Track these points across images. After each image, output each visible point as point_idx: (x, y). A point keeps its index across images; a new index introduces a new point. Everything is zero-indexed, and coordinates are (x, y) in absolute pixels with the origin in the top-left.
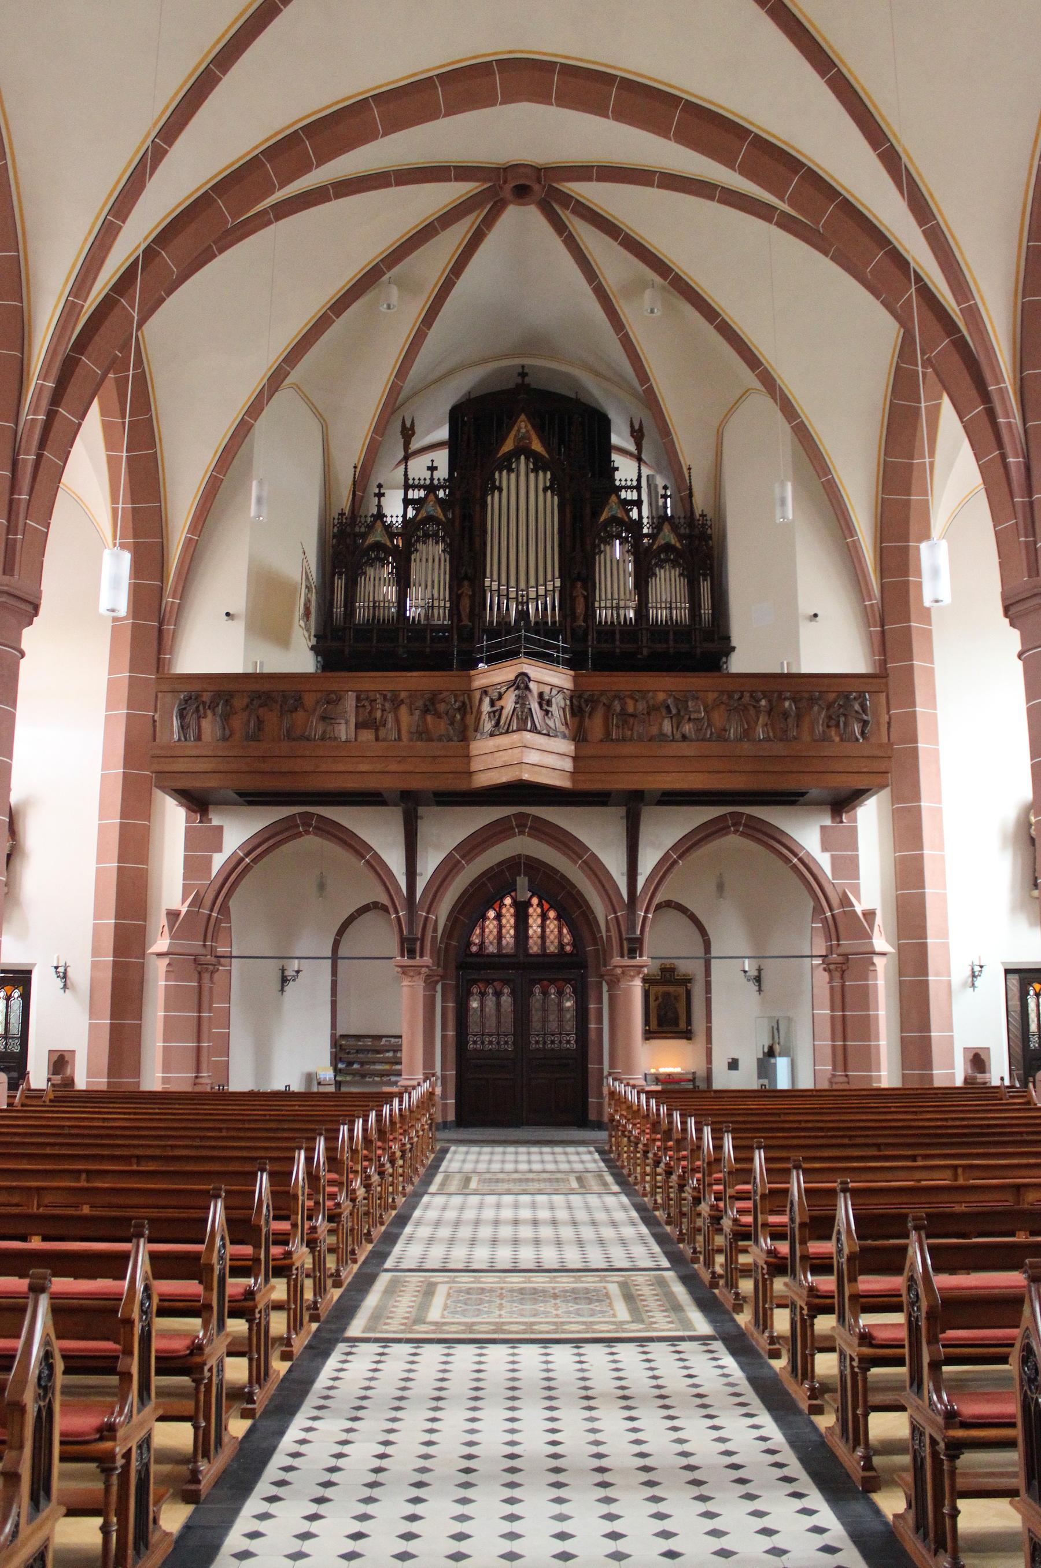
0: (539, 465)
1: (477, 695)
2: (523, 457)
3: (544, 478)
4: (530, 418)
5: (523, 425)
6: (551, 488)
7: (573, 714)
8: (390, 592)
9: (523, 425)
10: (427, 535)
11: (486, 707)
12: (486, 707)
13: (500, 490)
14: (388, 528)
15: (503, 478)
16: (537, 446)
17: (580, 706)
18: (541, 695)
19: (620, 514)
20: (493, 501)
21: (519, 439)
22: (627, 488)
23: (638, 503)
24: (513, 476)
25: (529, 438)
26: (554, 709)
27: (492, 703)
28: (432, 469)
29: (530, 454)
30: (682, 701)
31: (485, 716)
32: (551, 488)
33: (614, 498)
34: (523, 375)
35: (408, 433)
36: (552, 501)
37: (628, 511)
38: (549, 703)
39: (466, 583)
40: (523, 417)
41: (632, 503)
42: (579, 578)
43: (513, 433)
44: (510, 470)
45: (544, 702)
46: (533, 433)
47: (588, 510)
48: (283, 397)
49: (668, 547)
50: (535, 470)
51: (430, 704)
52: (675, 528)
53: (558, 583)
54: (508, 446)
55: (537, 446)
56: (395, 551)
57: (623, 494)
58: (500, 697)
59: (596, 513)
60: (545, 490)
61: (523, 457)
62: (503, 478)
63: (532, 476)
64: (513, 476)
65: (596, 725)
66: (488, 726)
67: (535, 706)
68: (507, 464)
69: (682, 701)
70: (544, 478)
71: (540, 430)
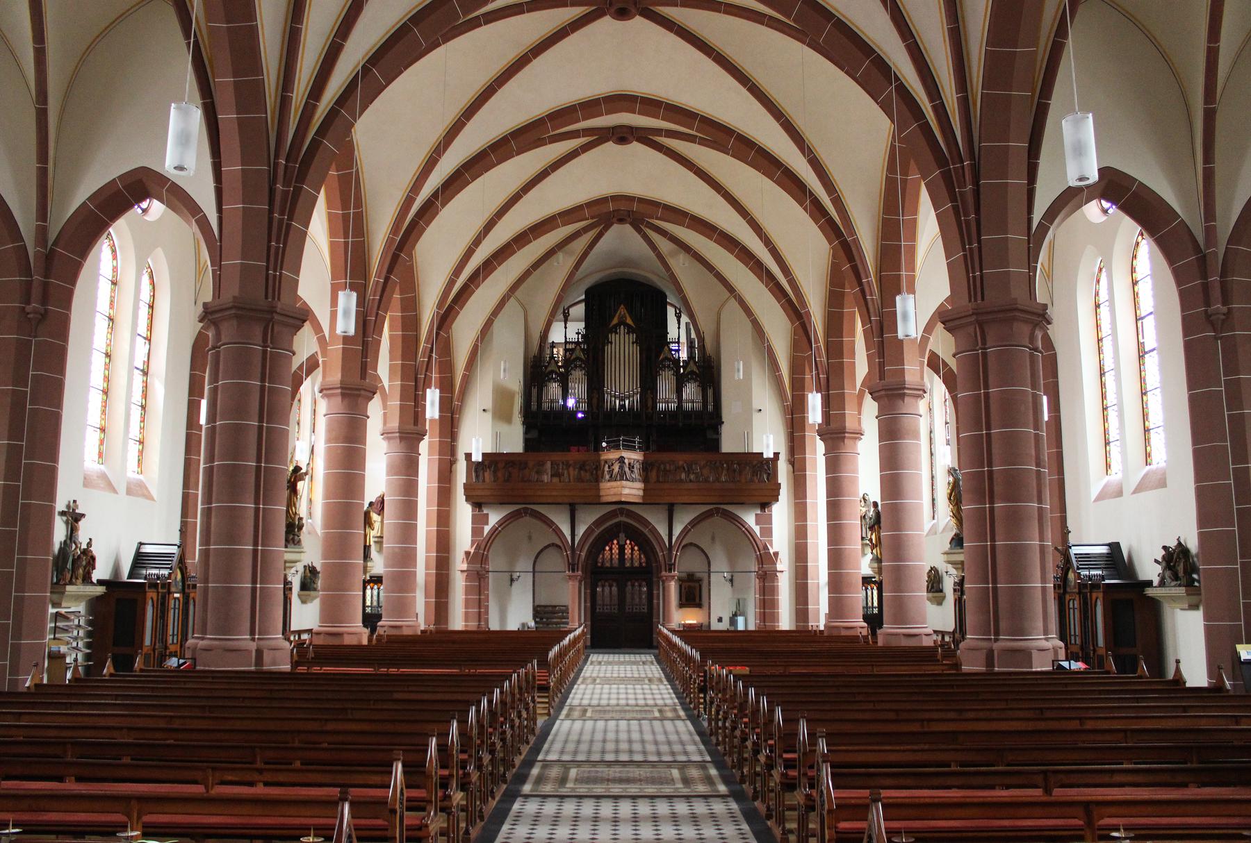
0: (630, 330)
3: (633, 337)
11: (606, 469)
12: (606, 469)
15: (612, 337)
16: (629, 321)
17: (646, 467)
20: (608, 348)
29: (626, 325)
45: (631, 467)
54: (615, 321)
55: (629, 321)
62: (612, 337)
65: (653, 474)
66: (607, 477)
67: (627, 470)
68: (614, 330)
70: (633, 337)
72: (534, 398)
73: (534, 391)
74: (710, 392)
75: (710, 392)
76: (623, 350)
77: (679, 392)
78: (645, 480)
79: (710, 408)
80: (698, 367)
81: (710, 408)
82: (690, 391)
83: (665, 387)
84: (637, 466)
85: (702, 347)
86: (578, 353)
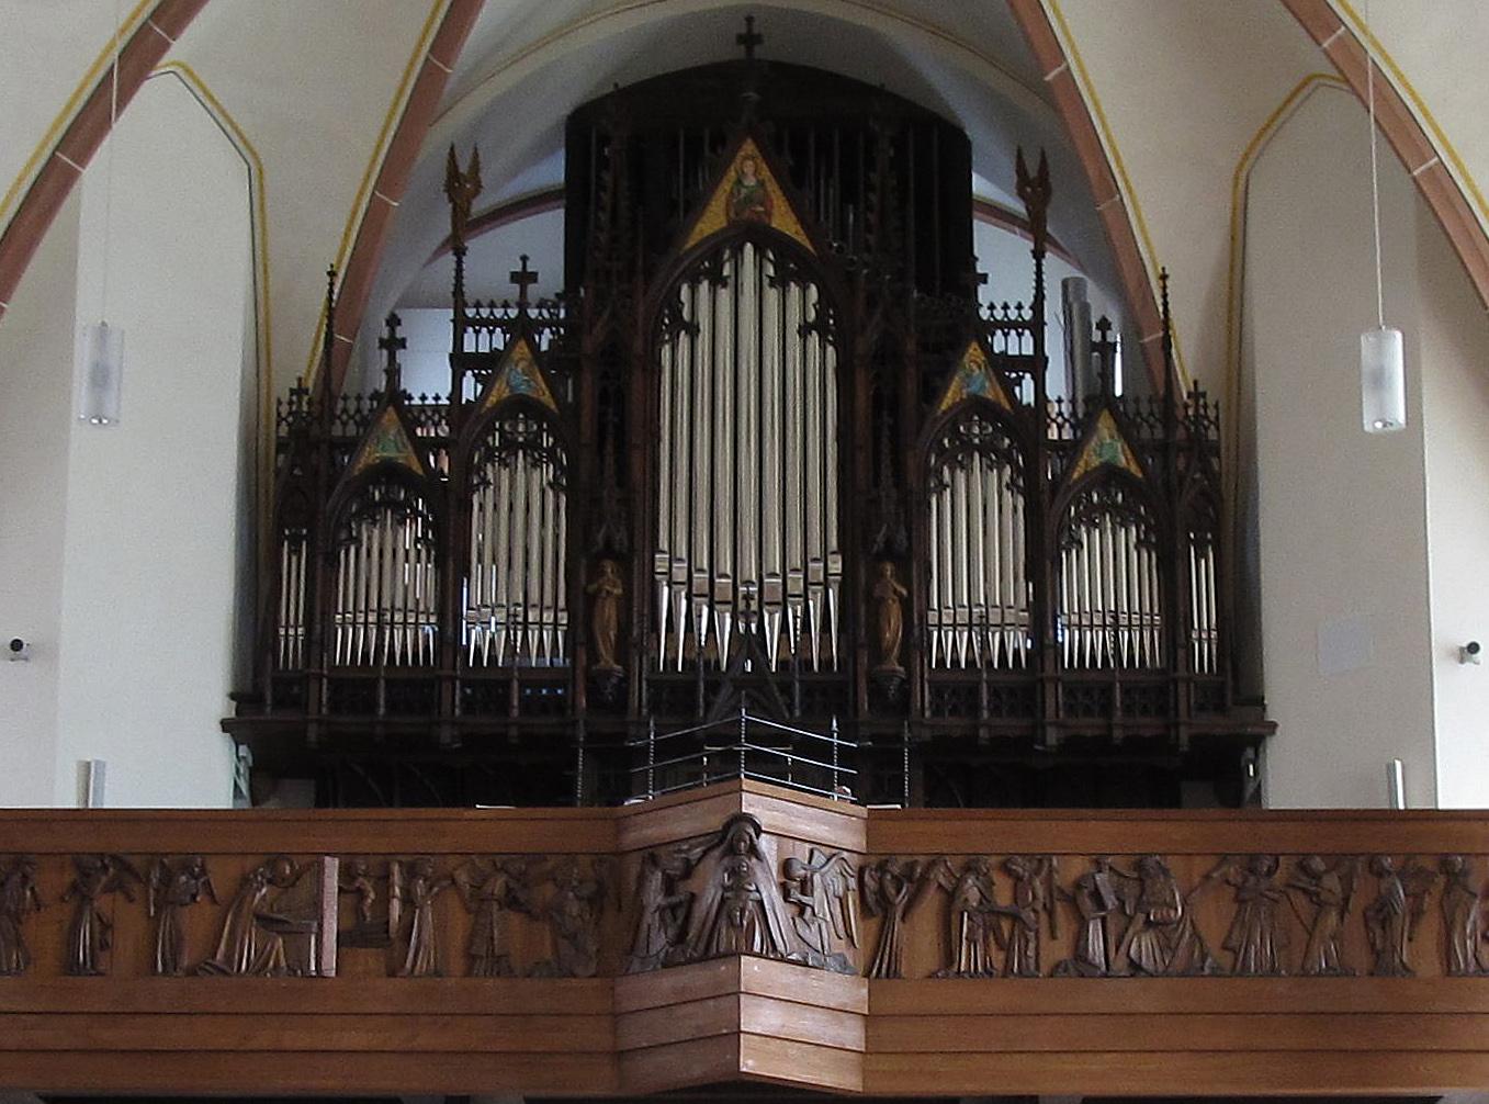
0: (790, 266)
1: (633, 867)
2: (749, 247)
3: (803, 301)
4: (770, 153)
5: (748, 169)
6: (820, 326)
7: (865, 910)
8: (416, 578)
9: (748, 169)
10: (510, 446)
11: (654, 896)
12: (654, 896)
13: (693, 330)
14: (410, 416)
15: (699, 301)
16: (784, 221)
17: (882, 891)
18: (786, 867)
19: (991, 392)
20: (675, 358)
21: (737, 205)
22: (1007, 326)
23: (1036, 364)
24: (725, 295)
25: (765, 201)
26: (817, 899)
27: (669, 886)
28: (524, 278)
29: (765, 239)
30: (1142, 871)
31: (651, 918)
32: (820, 326)
33: (974, 351)
34: (749, 39)
35: (460, 183)
36: (821, 357)
37: (1009, 387)
38: (806, 886)
39: (609, 567)
40: (749, 147)
41: (1021, 363)
42: (888, 552)
43: (726, 186)
44: (717, 281)
45: (794, 883)
46: (773, 188)
47: (911, 387)
48: (157, 93)
49: (1109, 475)
50: (781, 282)
51: (517, 886)
52: (1125, 428)
53: (836, 566)
54: (712, 220)
55: (784, 221)
56: (428, 484)
57: (998, 343)
58: (689, 870)
59: (931, 393)
60: (804, 331)
61: (749, 247)
62: (699, 301)
63: (772, 295)
64: (725, 295)
65: (919, 937)
66: (660, 942)
67: (771, 894)
68: (710, 267)
69: (1142, 871)
70: (803, 301)
71: (794, 182)
72: (292, 605)
73: (294, 568)
74: (1202, 574)
75: (1202, 574)
76: (750, 377)
77: (1041, 564)
78: (880, 966)
79: (1204, 650)
80: (1137, 450)
81: (1204, 650)
82: (1106, 576)
83: (974, 534)
84: (830, 884)
85: (1155, 353)
86: (521, 378)
